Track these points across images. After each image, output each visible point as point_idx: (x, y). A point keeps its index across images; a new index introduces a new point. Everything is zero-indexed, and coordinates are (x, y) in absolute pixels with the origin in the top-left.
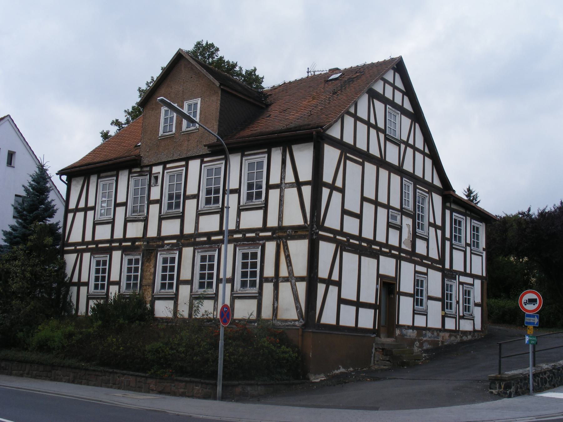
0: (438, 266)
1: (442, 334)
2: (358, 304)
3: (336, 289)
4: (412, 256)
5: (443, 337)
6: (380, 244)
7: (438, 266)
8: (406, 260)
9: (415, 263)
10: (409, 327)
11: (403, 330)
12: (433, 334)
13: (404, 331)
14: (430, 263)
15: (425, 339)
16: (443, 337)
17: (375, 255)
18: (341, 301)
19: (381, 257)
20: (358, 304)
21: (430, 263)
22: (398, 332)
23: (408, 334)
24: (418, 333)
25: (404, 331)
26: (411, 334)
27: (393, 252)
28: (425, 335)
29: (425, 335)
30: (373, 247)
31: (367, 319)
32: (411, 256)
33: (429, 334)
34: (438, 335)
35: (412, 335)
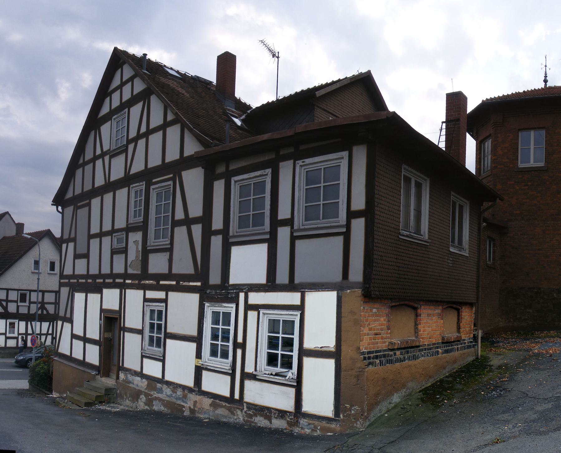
0: (191, 284)
1: (193, 397)
2: (85, 340)
3: (69, 325)
4: (142, 279)
5: (195, 402)
6: (105, 276)
7: (191, 284)
8: (131, 287)
9: (145, 288)
10: (135, 373)
11: (129, 375)
12: (174, 392)
13: (130, 378)
14: (174, 283)
15: (157, 395)
16: (195, 402)
17: (98, 289)
18: (74, 336)
19: (105, 291)
20: (85, 340)
21: (161, 282)
22: (122, 376)
23: (135, 382)
24: (148, 385)
25: (130, 378)
26: (140, 383)
27: (117, 281)
28: (160, 391)
29: (160, 391)
30: (98, 281)
31: (93, 355)
32: (140, 280)
33: (167, 391)
34: (185, 396)
35: (140, 384)
